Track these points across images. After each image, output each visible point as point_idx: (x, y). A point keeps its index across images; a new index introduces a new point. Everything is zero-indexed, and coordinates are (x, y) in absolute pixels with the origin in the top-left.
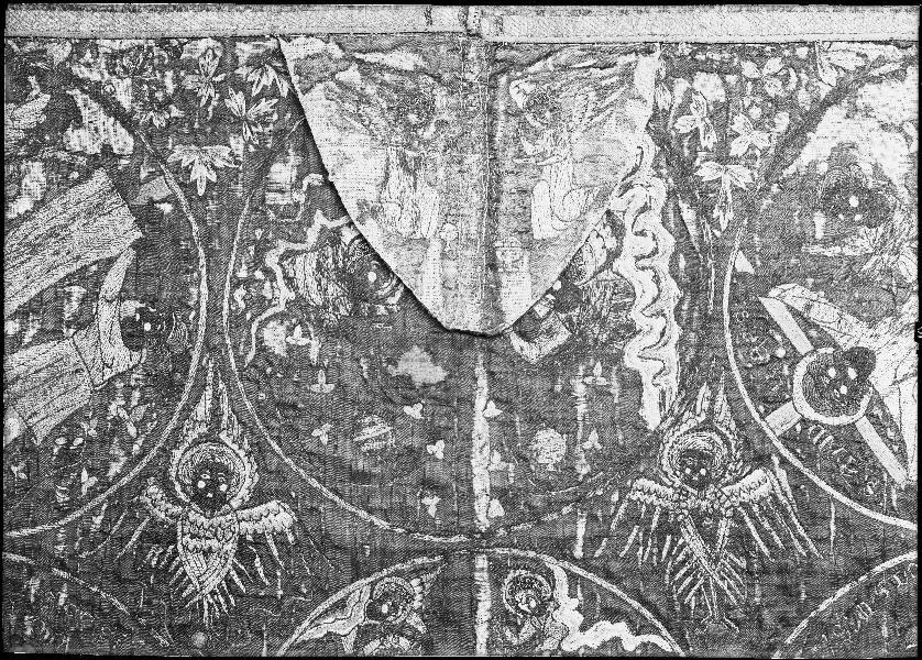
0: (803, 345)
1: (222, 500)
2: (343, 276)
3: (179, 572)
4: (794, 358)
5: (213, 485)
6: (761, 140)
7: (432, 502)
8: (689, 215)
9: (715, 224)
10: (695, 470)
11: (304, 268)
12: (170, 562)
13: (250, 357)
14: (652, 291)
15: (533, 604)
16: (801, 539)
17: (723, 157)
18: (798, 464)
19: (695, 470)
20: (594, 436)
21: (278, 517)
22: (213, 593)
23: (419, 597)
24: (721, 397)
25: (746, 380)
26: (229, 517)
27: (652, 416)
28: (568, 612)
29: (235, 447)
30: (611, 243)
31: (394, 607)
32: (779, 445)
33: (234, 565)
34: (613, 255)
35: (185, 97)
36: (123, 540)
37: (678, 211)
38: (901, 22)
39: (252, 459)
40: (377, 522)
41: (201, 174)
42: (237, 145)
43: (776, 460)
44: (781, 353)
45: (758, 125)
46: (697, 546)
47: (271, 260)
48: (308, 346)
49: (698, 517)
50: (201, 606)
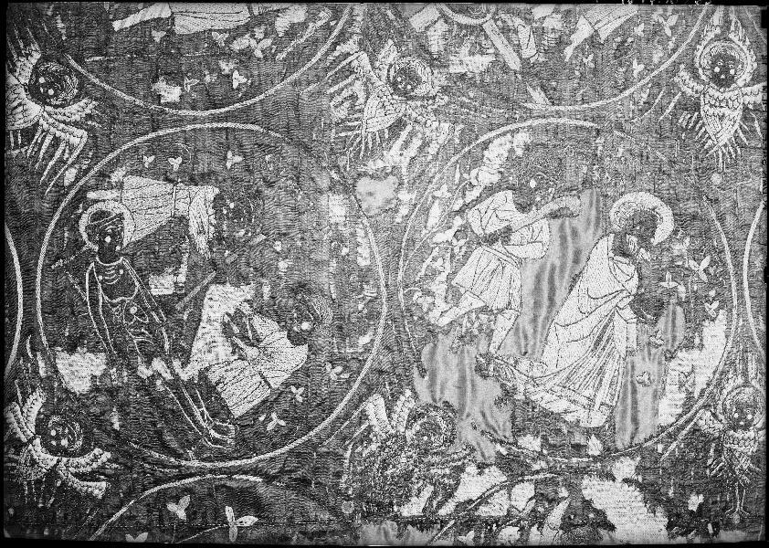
5: (725, 70)
12: (694, 127)
22: (725, 146)
26: (736, 92)
29: (740, 44)
36: (662, 109)
39: (752, 53)
50: (718, 156)
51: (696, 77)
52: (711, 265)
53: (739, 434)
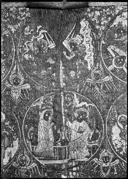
0: (114, 55)
1: (18, 84)
2: (38, 46)
3: (12, 96)
4: (113, 58)
5: (17, 81)
6: (106, 22)
7: (53, 83)
8: (94, 34)
9: (99, 36)
10: (97, 77)
11: (31, 45)
12: (10, 94)
13: (22, 60)
14: (89, 47)
15: (71, 100)
16: (114, 87)
17: (100, 24)
18: (114, 75)
19: (97, 77)
20: (80, 72)
21: (28, 86)
23: (52, 99)
24: (101, 64)
25: (104, 61)
27: (89, 68)
28: (76, 100)
29: (20, 75)
30: (82, 39)
31: (47, 101)
32: (110, 72)
33: (21, 94)
34: (82, 41)
35: (10, 17)
37: (93, 34)
38: (126, 3)
40: (45, 87)
41: (13, 30)
42: (19, 25)
43: (110, 75)
44: (110, 57)
45: (106, 19)
46: (97, 89)
47: (25, 44)
48: (32, 58)
49: (97, 84)
51: (10, 83)
52: (15, 127)
53: (22, 167)
